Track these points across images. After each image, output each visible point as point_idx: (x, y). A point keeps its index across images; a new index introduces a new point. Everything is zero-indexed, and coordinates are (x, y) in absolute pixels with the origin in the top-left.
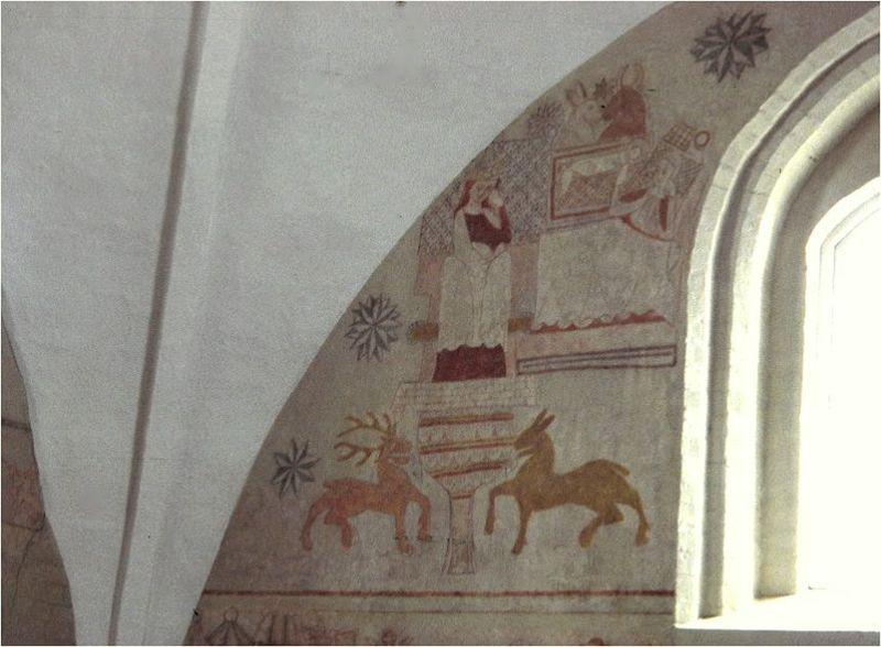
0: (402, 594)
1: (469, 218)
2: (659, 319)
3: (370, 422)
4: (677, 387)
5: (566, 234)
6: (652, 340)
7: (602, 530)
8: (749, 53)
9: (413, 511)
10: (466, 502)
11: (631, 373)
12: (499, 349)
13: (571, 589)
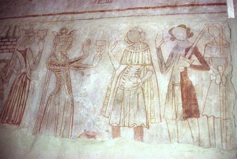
13: (166, 5)
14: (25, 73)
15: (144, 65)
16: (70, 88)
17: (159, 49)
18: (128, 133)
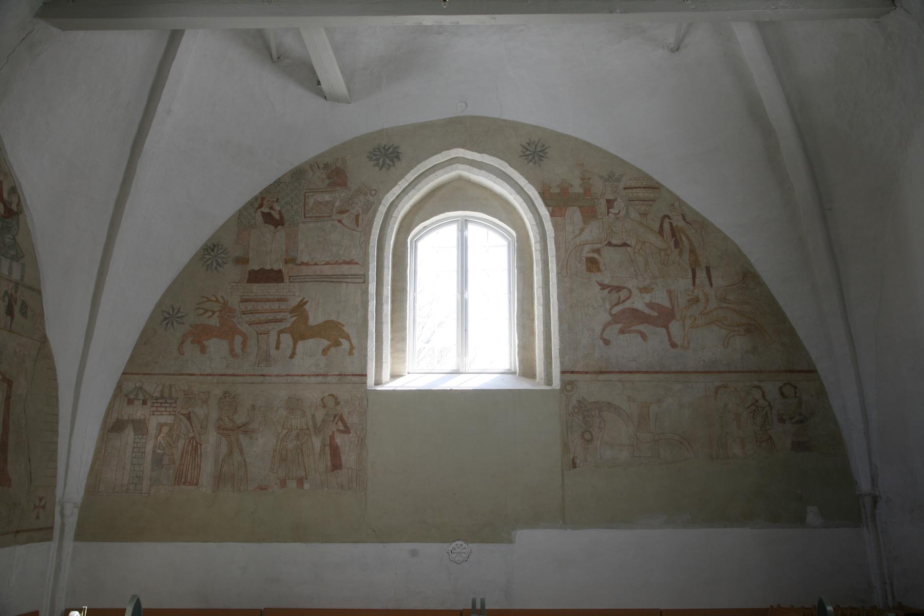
0: (234, 375)
1: (263, 214)
2: (357, 263)
3: (214, 299)
4: (366, 292)
5: (311, 225)
6: (353, 272)
7: (332, 349)
8: (392, 161)
9: (238, 339)
10: (265, 336)
11: (344, 285)
12: (280, 271)
14: (194, 438)
15: (302, 429)
16: (241, 451)
17: (313, 416)
18: (292, 484)
